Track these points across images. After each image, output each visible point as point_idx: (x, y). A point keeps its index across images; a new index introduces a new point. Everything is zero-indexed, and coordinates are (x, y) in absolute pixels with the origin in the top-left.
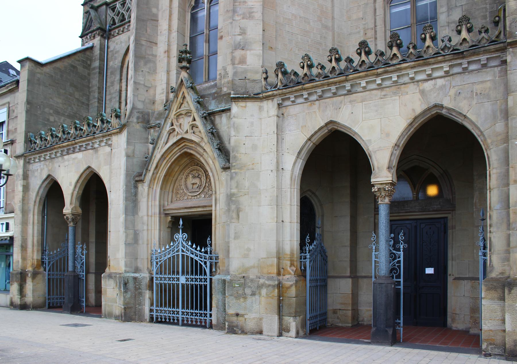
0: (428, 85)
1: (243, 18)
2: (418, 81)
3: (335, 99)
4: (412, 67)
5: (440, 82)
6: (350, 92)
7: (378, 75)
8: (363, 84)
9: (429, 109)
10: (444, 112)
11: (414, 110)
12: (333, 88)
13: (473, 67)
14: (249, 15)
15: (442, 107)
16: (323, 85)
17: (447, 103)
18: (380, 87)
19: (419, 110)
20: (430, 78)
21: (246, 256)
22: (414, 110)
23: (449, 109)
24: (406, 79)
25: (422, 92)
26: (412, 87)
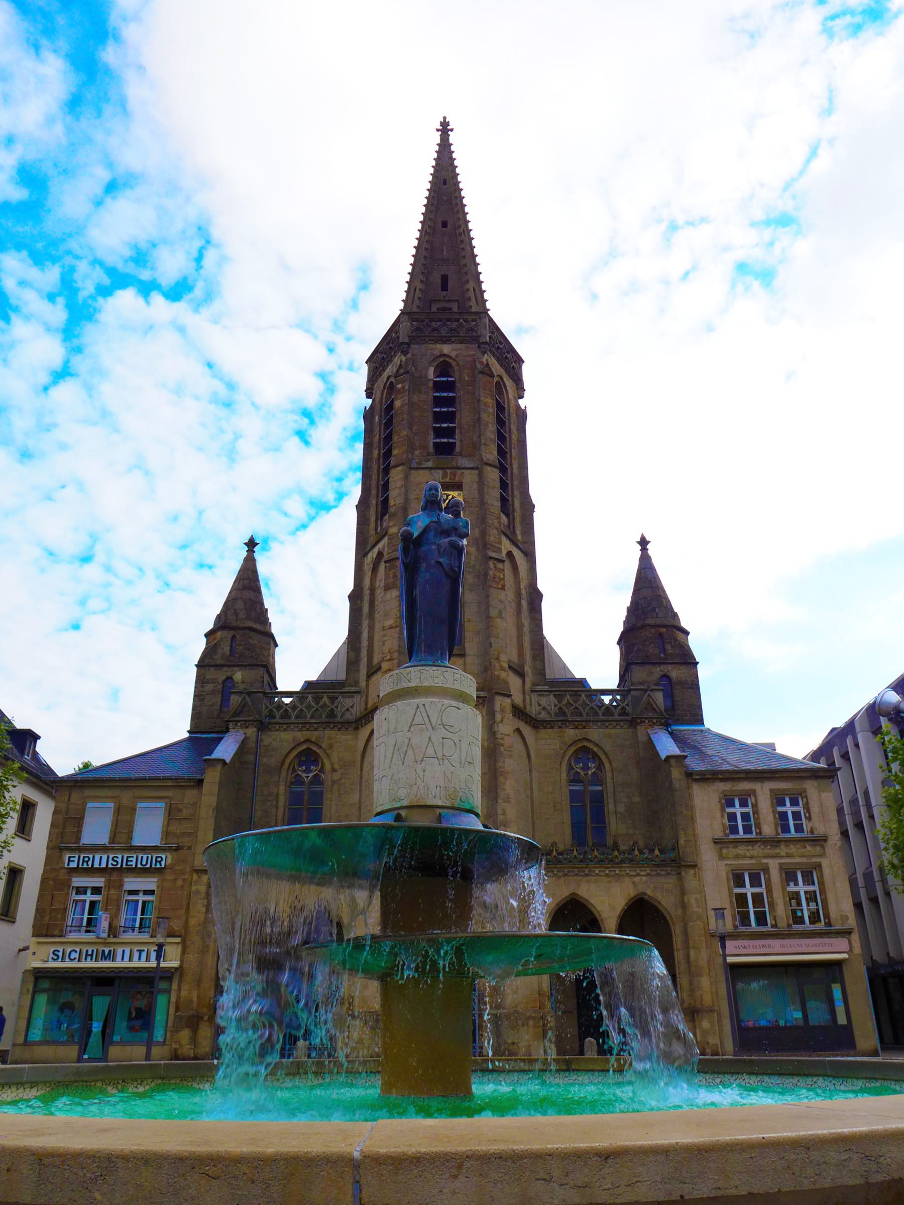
0: (637, 879)
1: (504, 802)
2: (631, 876)
3: (576, 878)
4: (628, 867)
5: (644, 878)
6: (587, 875)
7: (607, 868)
8: (597, 871)
9: (638, 894)
10: (646, 897)
11: (629, 894)
12: (576, 871)
13: (663, 873)
14: (507, 800)
15: (646, 894)
16: (569, 868)
17: (649, 892)
18: (607, 875)
19: (632, 895)
20: (638, 875)
21: (516, 993)
22: (629, 894)
23: (649, 896)
24: (623, 873)
25: (634, 883)
26: (627, 879)
